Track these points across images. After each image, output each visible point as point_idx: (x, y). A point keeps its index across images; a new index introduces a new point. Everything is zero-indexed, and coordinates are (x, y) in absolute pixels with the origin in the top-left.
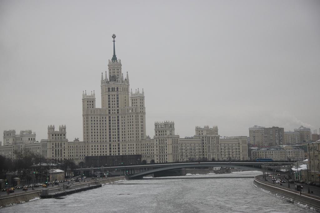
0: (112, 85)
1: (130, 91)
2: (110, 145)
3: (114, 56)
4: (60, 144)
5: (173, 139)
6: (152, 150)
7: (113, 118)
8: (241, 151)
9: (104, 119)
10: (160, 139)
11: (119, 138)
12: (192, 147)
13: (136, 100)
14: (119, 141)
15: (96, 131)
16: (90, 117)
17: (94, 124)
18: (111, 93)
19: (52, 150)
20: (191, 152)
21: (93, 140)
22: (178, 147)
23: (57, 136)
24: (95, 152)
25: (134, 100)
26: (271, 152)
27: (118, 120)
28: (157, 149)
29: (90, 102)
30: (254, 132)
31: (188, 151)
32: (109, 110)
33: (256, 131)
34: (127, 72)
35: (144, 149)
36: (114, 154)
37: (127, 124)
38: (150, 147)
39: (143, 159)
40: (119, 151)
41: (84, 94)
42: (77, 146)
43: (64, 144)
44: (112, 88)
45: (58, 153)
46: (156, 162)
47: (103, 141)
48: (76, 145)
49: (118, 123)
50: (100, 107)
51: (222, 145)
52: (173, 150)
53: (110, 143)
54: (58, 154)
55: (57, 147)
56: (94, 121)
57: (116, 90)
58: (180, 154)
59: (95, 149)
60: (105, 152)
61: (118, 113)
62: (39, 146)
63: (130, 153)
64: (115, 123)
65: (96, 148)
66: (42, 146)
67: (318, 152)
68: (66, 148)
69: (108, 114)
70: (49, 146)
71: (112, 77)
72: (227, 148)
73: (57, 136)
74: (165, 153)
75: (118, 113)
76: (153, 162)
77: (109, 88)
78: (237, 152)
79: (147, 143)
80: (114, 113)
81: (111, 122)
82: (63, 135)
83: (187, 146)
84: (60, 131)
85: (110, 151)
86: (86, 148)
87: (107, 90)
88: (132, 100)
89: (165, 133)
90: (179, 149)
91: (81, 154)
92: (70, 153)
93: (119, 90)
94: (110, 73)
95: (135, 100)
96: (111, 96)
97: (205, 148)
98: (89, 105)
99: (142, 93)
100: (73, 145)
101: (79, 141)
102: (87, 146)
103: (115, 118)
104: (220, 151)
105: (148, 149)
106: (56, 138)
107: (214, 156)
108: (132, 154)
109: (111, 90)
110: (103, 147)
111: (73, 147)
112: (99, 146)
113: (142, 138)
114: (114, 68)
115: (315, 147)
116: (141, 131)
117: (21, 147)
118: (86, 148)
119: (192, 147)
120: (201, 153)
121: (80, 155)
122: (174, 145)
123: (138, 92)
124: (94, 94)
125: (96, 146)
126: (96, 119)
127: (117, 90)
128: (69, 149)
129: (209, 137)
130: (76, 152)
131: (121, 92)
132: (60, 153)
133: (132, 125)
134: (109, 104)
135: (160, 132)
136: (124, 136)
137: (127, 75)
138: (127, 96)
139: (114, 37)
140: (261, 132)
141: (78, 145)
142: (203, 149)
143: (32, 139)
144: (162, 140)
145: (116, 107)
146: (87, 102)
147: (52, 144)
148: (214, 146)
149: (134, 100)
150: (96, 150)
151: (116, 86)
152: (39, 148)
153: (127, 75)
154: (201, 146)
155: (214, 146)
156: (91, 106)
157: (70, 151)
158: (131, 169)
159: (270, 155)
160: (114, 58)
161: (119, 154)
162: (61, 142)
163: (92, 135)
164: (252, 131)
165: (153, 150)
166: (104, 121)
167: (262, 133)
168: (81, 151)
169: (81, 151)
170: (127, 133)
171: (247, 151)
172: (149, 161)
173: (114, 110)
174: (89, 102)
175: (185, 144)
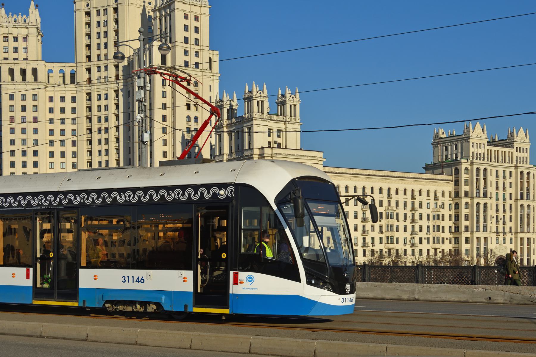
12: (401, 205)
29: (16, 39)
32: (89, 70)
96: (94, 13)
97: (464, 211)
98: (11, 50)
119: (401, 205)
120: (446, 234)
126: (29, 103)
129: (485, 170)
154: (447, 206)
156: (21, 55)
166: (68, 110)
173: (103, 68)
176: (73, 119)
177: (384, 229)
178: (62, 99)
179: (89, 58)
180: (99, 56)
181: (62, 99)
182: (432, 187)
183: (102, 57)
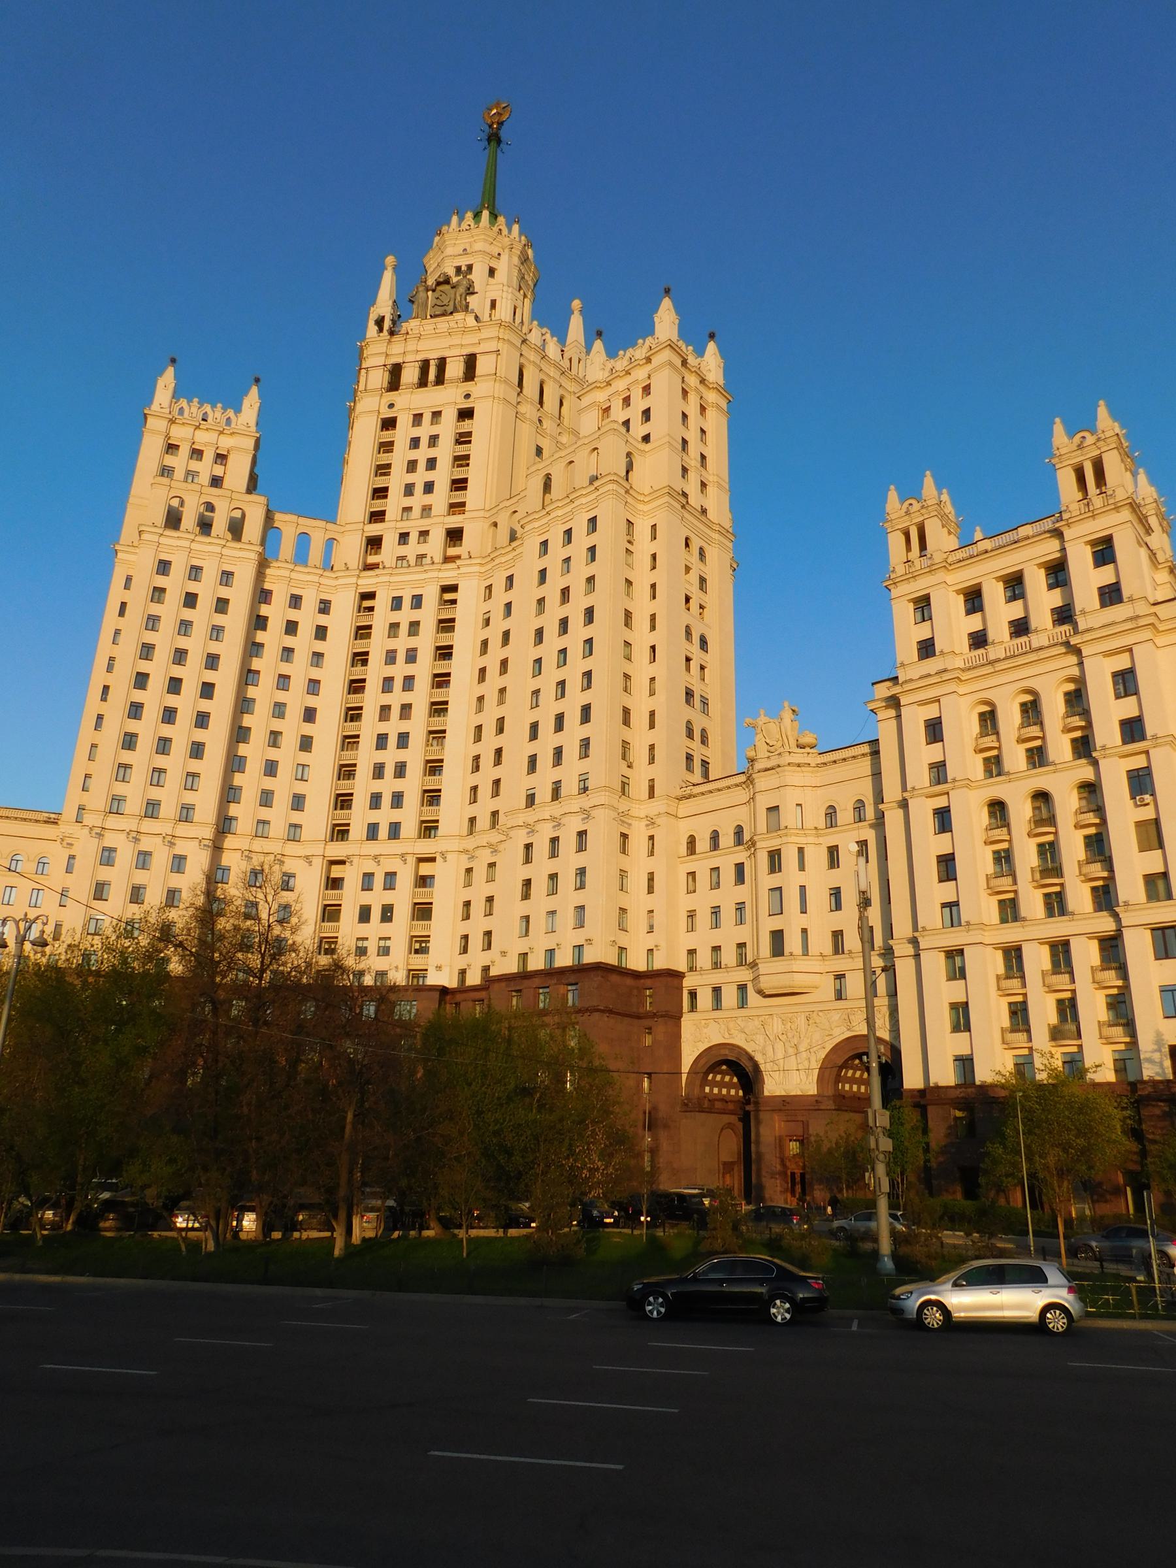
14: (428, 829)
15: (187, 703)
18: (409, 400)
35: (729, 894)
38: (817, 857)
40: (420, 946)
53: (337, 850)
71: (439, 284)
77: (396, 372)
87: (377, 378)
93: (482, 366)
103: (417, 601)
108: (564, 959)
109: (410, 375)
126: (207, 589)
151: (456, 340)
174: (184, 451)
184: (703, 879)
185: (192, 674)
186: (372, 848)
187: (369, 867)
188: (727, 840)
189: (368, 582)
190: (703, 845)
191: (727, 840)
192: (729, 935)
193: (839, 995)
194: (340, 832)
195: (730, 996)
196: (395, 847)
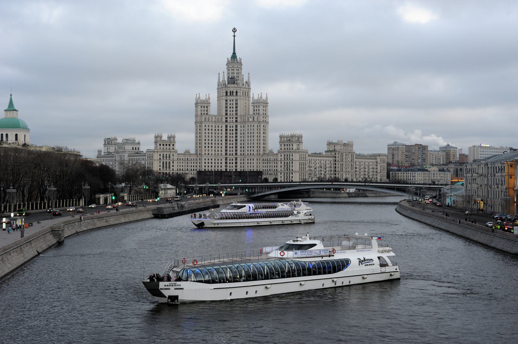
0: (232, 88)
1: (251, 96)
2: (226, 159)
3: (234, 53)
4: (168, 156)
5: (301, 154)
6: (276, 166)
7: (230, 127)
8: (379, 171)
9: (220, 129)
10: (286, 154)
11: (236, 150)
13: (258, 107)
16: (203, 125)
17: (209, 133)
18: (229, 98)
19: (159, 161)
20: (321, 171)
21: (207, 152)
22: (306, 164)
23: (165, 147)
24: (208, 166)
25: (255, 107)
26: (413, 173)
27: (236, 130)
28: (281, 166)
29: (204, 107)
30: (393, 149)
31: (317, 169)
33: (395, 148)
34: (249, 74)
35: (266, 165)
36: (230, 170)
37: (247, 135)
38: (273, 163)
39: (264, 177)
40: (236, 166)
41: (198, 97)
42: (188, 158)
43: (173, 155)
44: (231, 91)
45: (166, 165)
46: (279, 181)
47: (218, 154)
48: (186, 158)
49: (236, 133)
50: (216, 114)
51: (358, 163)
52: (300, 168)
53: (226, 156)
54: (166, 167)
55: (165, 158)
56: (209, 130)
57: (235, 94)
58: (308, 172)
59: (208, 163)
60: (220, 167)
61: (236, 121)
62: (144, 157)
63: (249, 168)
64: (233, 134)
65: (210, 161)
66: (148, 157)
67: (477, 175)
68: (175, 160)
69: (225, 121)
70: (156, 156)
72: (362, 167)
73: (165, 147)
74: (291, 170)
75: (236, 121)
76: (276, 180)
77: (227, 92)
78: (373, 171)
79: (269, 158)
80: (231, 121)
81: (228, 132)
82: (172, 145)
83: (316, 164)
84: (169, 140)
85: (226, 166)
86: (199, 161)
87: (225, 94)
88: (253, 107)
89: (291, 147)
90: (307, 167)
91: (192, 168)
92: (179, 166)
93: (238, 94)
94: (228, 74)
95: (257, 107)
96: (229, 100)
97: (337, 166)
98: (203, 110)
99: (265, 99)
100: (183, 157)
101: (190, 152)
102: (199, 159)
103: (233, 127)
104: (354, 171)
105: (271, 165)
106: (163, 148)
107: (348, 176)
109: (229, 94)
110: (218, 161)
111: (183, 159)
112: (213, 159)
113: (264, 152)
114: (233, 68)
115: (474, 169)
116: (263, 143)
117: (124, 157)
118: (199, 161)
120: (332, 172)
121: (191, 169)
122: (301, 162)
123: (261, 97)
124: (209, 98)
125: (210, 159)
126: (210, 128)
127: (237, 94)
128: (179, 162)
130: (186, 166)
131: (240, 96)
132: (168, 166)
133: (252, 137)
134: (226, 111)
135: (285, 146)
136: (242, 149)
137: (249, 76)
138: (247, 102)
139: (234, 30)
140: (401, 150)
141: (188, 157)
142: (335, 167)
143: (136, 148)
144: (287, 155)
145: (234, 114)
146: (200, 107)
147: (159, 155)
148: (348, 164)
149: (255, 107)
150: (210, 165)
151: (234, 89)
152: (144, 159)
153: (249, 76)
154: (333, 164)
155: (348, 164)
157: (179, 164)
158: (252, 187)
159: (412, 176)
160: (234, 56)
161: (236, 170)
162: (170, 153)
163: (205, 147)
164: (391, 148)
165: (277, 166)
166: (220, 130)
167: (402, 151)
168: (193, 165)
169: (193, 165)
170: (247, 146)
171: (386, 172)
172: (271, 179)
173: (231, 118)
175: (314, 160)
176: (221, 133)
177: (319, 171)
178: (218, 127)
179: (226, 114)
180: (230, 114)
181: (218, 127)
182: (330, 159)
183: (231, 114)
184: (264, 163)
185: (210, 138)
186: (230, 156)
187: (230, 158)
188: (266, 160)
189: (227, 124)
190: (264, 160)
191: (266, 160)
192: (266, 168)
193: (275, 174)
194: (226, 154)
195: (266, 174)
196: (232, 156)
